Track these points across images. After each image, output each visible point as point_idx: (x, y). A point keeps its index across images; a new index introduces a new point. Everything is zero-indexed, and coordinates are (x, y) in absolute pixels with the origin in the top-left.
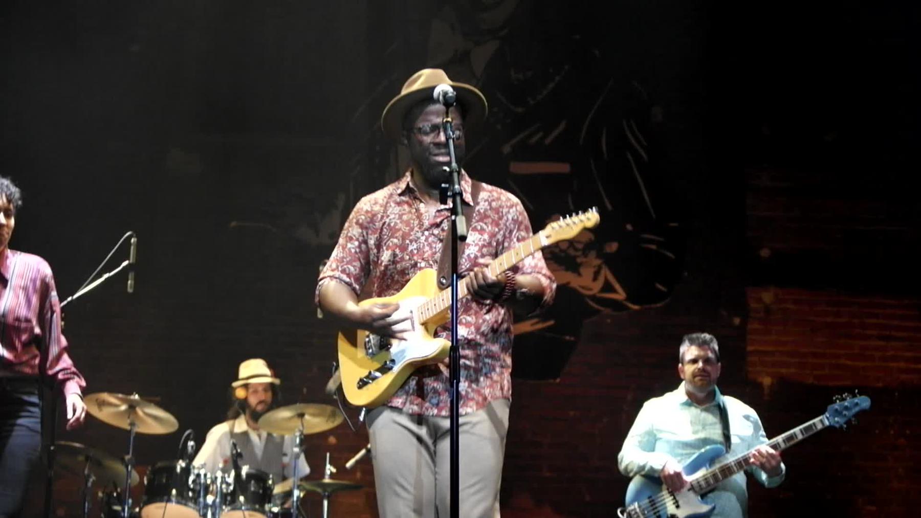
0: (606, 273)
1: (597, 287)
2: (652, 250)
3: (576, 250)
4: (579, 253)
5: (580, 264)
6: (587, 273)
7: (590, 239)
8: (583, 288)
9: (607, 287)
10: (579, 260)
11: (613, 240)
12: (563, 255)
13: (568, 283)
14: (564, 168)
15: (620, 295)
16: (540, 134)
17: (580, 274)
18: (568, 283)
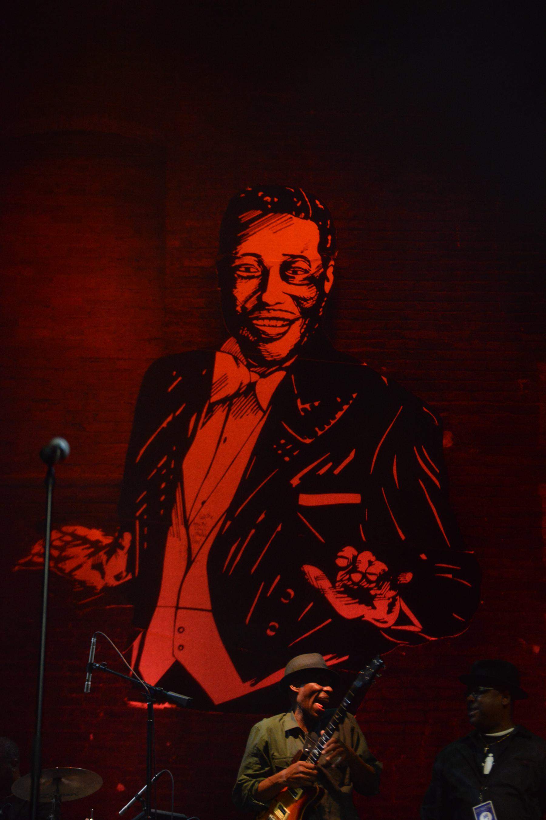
0: (400, 604)
1: (392, 619)
2: (449, 578)
3: (370, 582)
4: (373, 585)
5: (375, 596)
6: (381, 605)
7: (384, 570)
8: (378, 621)
9: (403, 619)
10: (373, 592)
11: (406, 571)
12: (356, 587)
13: (363, 616)
14: (354, 498)
15: (416, 627)
16: (330, 464)
17: (374, 608)
18: (363, 616)
